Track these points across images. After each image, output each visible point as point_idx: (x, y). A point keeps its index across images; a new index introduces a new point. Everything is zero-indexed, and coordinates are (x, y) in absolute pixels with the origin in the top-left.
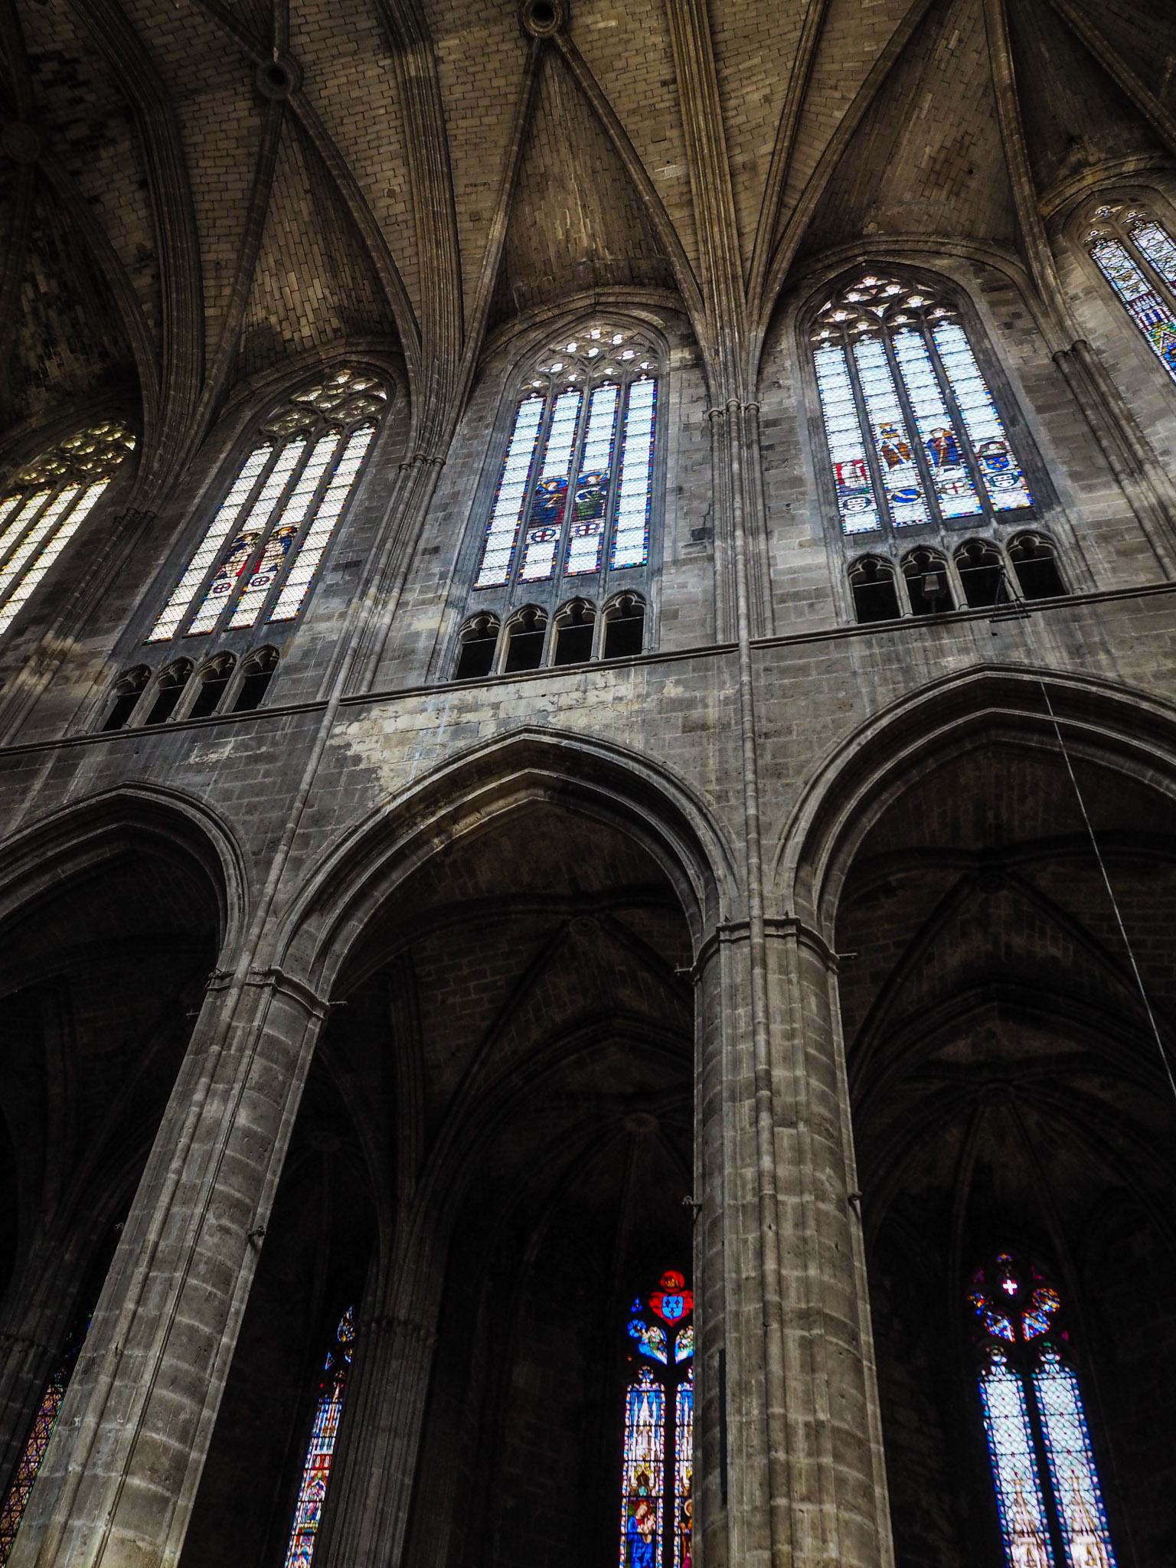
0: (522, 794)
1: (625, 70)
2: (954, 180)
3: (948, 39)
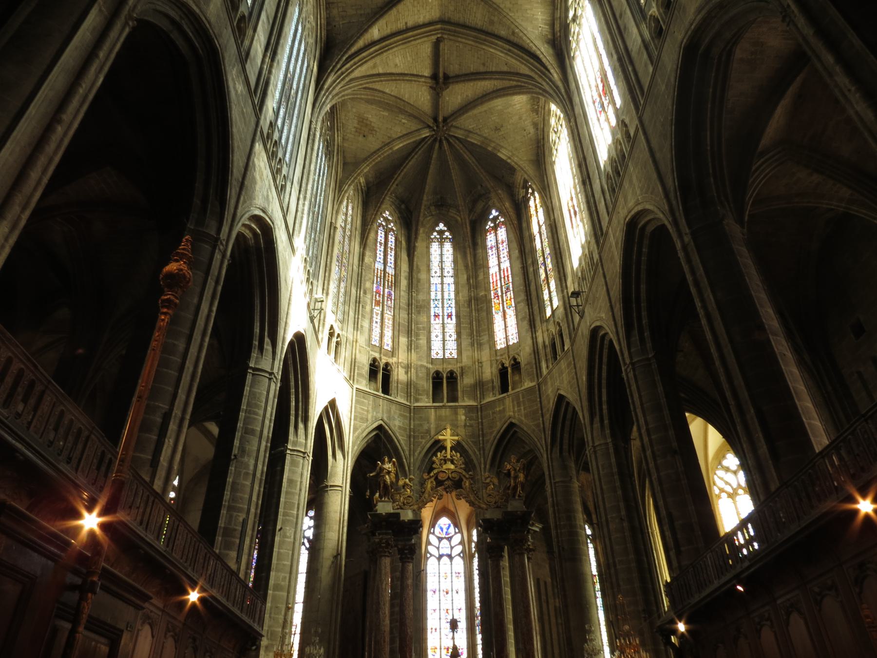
0: (248, 231)
1: (414, 6)
2: (360, 129)
3: (405, 119)
